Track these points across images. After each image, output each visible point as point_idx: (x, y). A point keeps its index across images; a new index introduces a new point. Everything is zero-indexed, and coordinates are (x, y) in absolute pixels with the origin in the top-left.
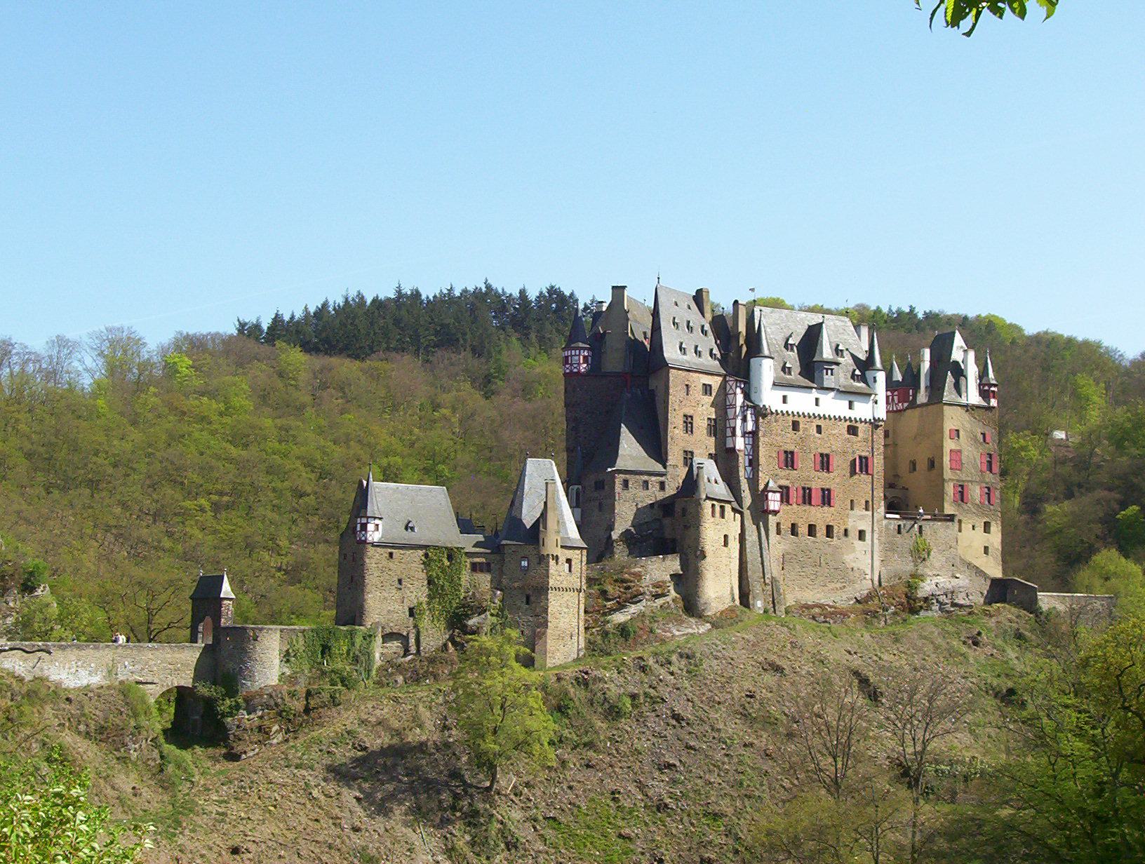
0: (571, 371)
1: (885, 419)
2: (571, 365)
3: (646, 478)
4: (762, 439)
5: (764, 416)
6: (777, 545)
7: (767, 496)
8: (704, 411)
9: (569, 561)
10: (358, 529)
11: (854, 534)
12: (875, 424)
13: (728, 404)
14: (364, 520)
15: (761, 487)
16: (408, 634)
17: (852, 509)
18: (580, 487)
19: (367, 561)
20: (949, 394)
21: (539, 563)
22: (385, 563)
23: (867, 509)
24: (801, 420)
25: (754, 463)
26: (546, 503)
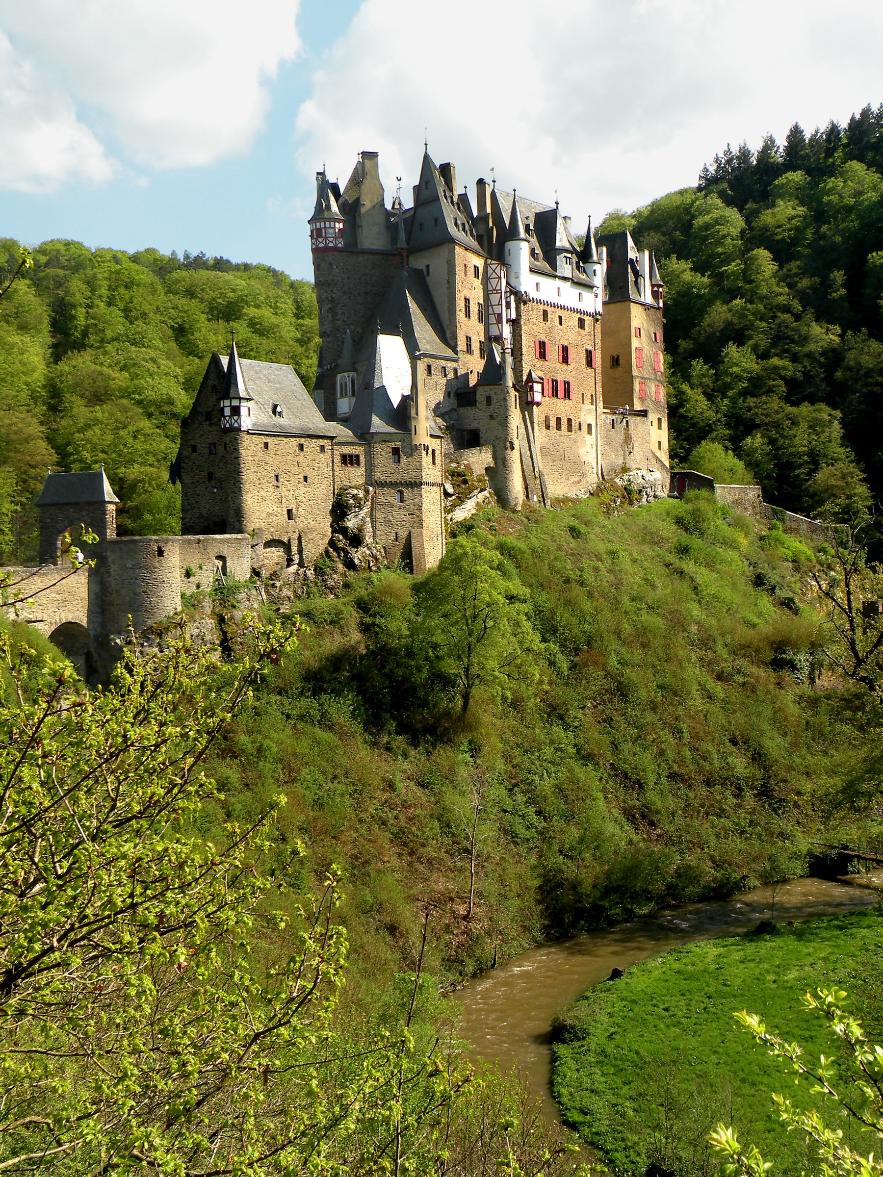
0: (326, 245)
1: (601, 311)
2: (326, 238)
3: (443, 363)
4: (523, 327)
5: (525, 303)
6: (540, 436)
7: (532, 388)
8: (477, 296)
9: (433, 451)
10: (227, 411)
11: (585, 428)
12: (595, 317)
13: (490, 288)
14: (235, 403)
15: (525, 378)
16: (289, 540)
17: (583, 403)
18: (355, 374)
19: (242, 452)
20: (632, 294)
21: (411, 455)
22: (260, 454)
23: (592, 404)
24: (549, 309)
25: (517, 352)
26: (414, 386)
